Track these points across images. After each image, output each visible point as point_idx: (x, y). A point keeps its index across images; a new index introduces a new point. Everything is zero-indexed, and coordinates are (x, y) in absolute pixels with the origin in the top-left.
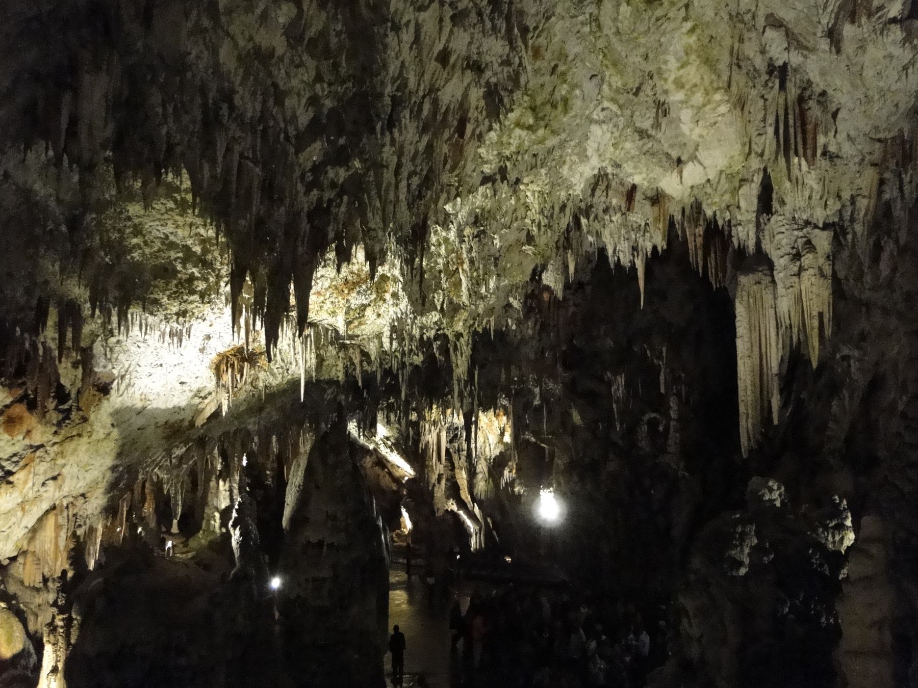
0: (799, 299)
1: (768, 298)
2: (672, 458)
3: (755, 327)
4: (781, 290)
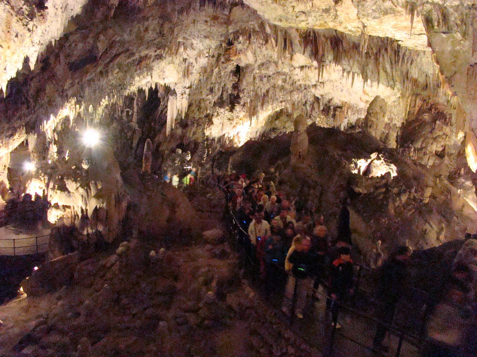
0: (182, 104)
1: (175, 102)
2: (134, 124)
3: (172, 108)
4: (178, 101)
